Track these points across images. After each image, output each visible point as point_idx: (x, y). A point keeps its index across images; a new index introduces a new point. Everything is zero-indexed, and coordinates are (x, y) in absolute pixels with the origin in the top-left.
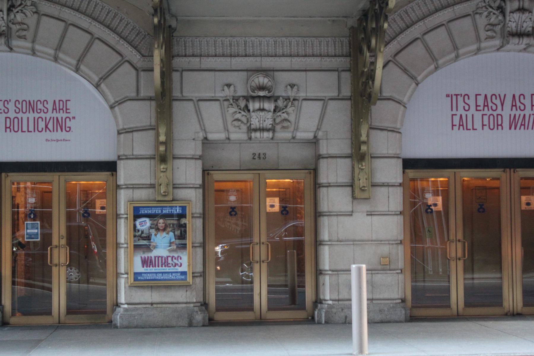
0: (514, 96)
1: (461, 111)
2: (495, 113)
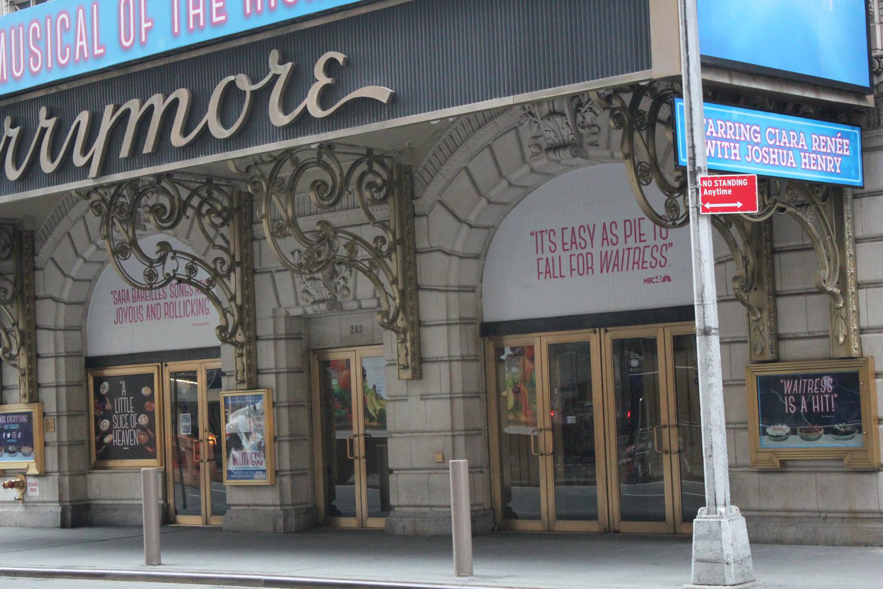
0: (604, 224)
1: (547, 254)
2: (584, 252)
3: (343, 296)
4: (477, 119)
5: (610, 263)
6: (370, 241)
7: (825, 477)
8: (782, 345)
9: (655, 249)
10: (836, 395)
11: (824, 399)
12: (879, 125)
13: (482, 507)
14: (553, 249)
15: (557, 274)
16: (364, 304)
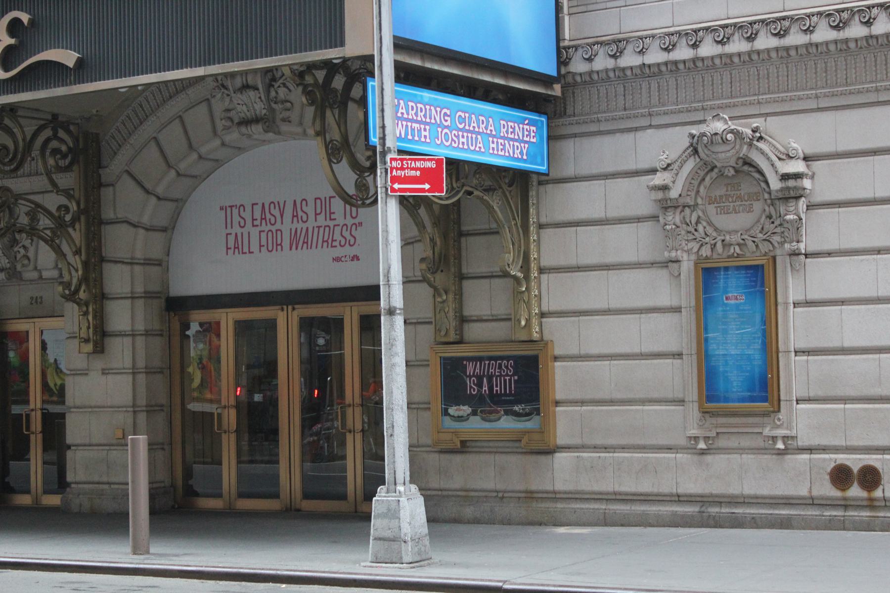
0: (295, 201)
1: (237, 229)
2: (274, 228)
3: (23, 265)
4: (168, 89)
5: (299, 241)
6: (53, 210)
7: (504, 457)
8: (466, 326)
9: (345, 228)
10: (516, 378)
11: (505, 381)
12: (565, 114)
13: (163, 485)
14: (242, 224)
15: (246, 250)
16: (45, 274)
